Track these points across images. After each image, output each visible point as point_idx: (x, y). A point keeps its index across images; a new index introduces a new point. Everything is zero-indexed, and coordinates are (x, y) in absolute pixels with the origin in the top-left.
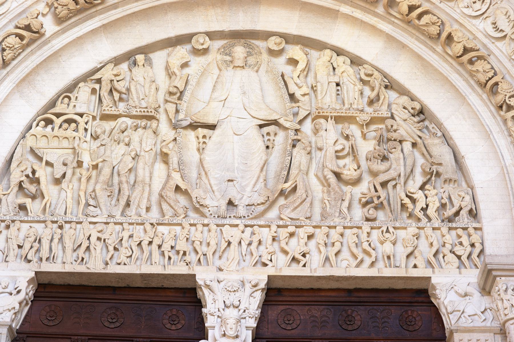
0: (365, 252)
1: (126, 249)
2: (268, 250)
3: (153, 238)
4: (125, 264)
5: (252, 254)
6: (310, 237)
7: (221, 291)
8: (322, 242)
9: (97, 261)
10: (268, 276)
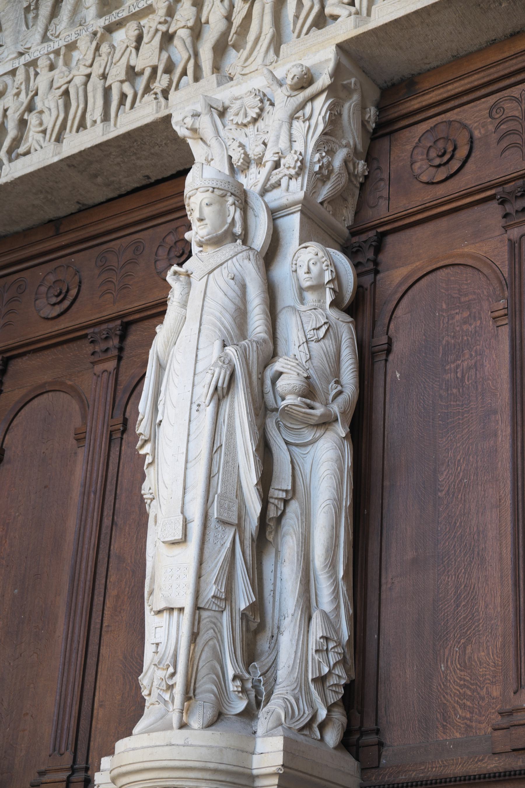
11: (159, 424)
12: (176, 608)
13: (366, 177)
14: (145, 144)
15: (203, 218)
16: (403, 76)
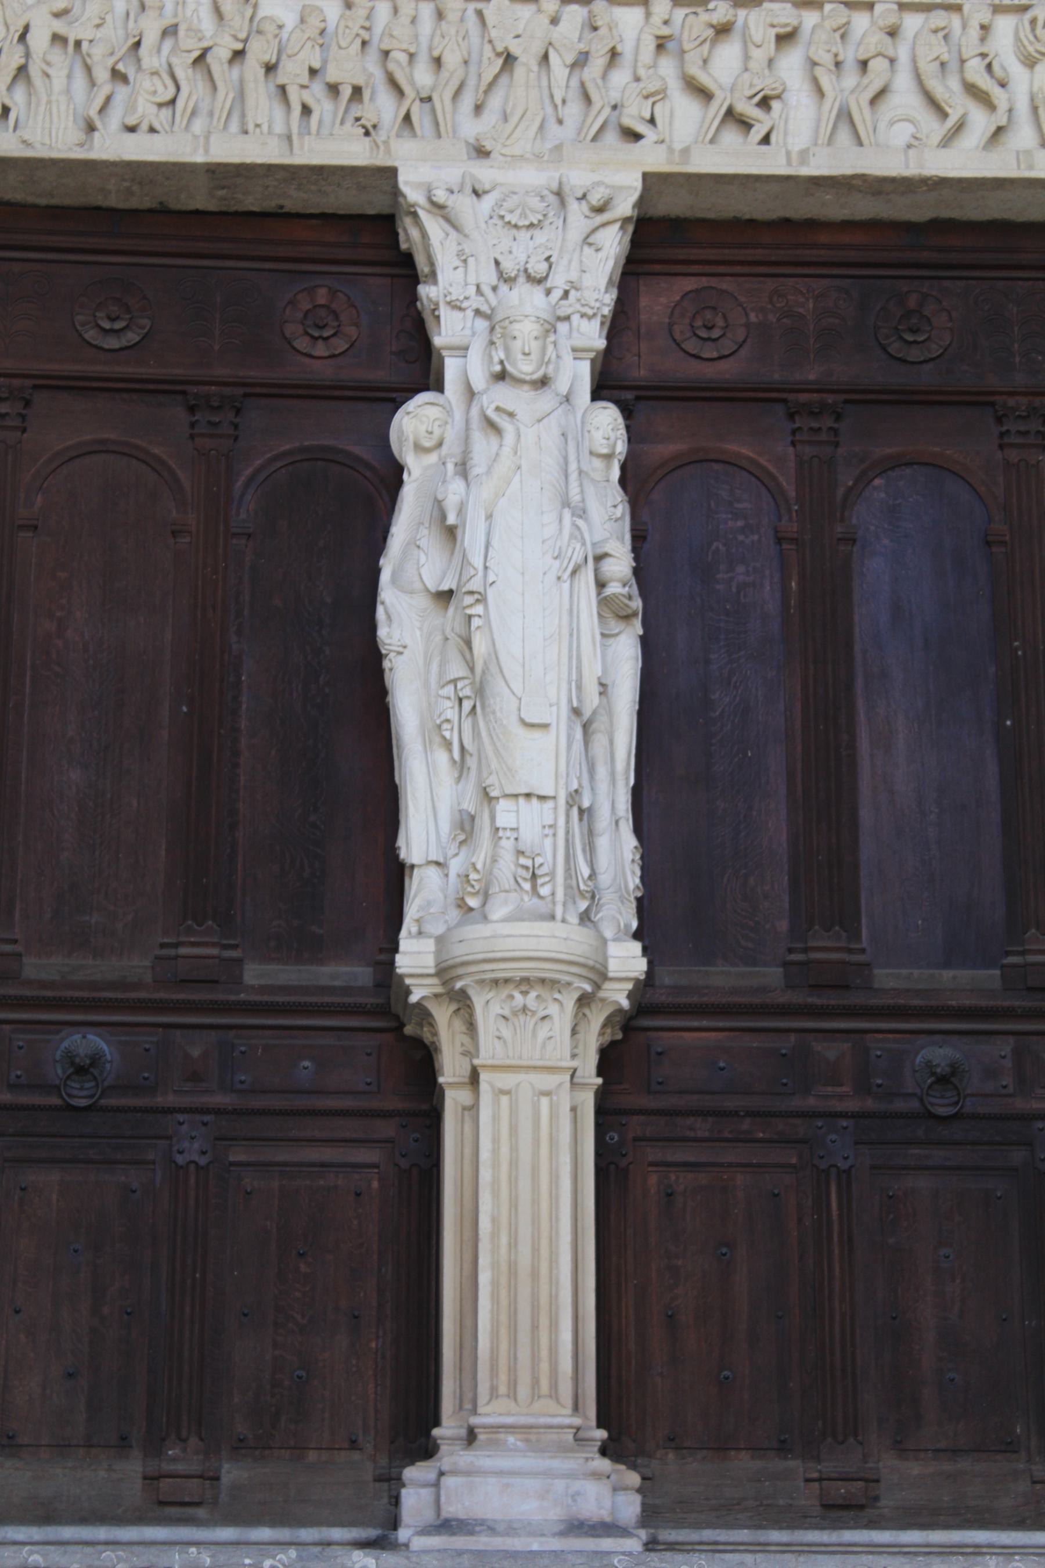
0: (972, 90)
1: (156, 79)
2: (642, 85)
3: (245, 41)
4: (152, 130)
5: (587, 99)
6: (786, 38)
7: (483, 226)
8: (827, 59)
9: (55, 119)
10: (646, 176)
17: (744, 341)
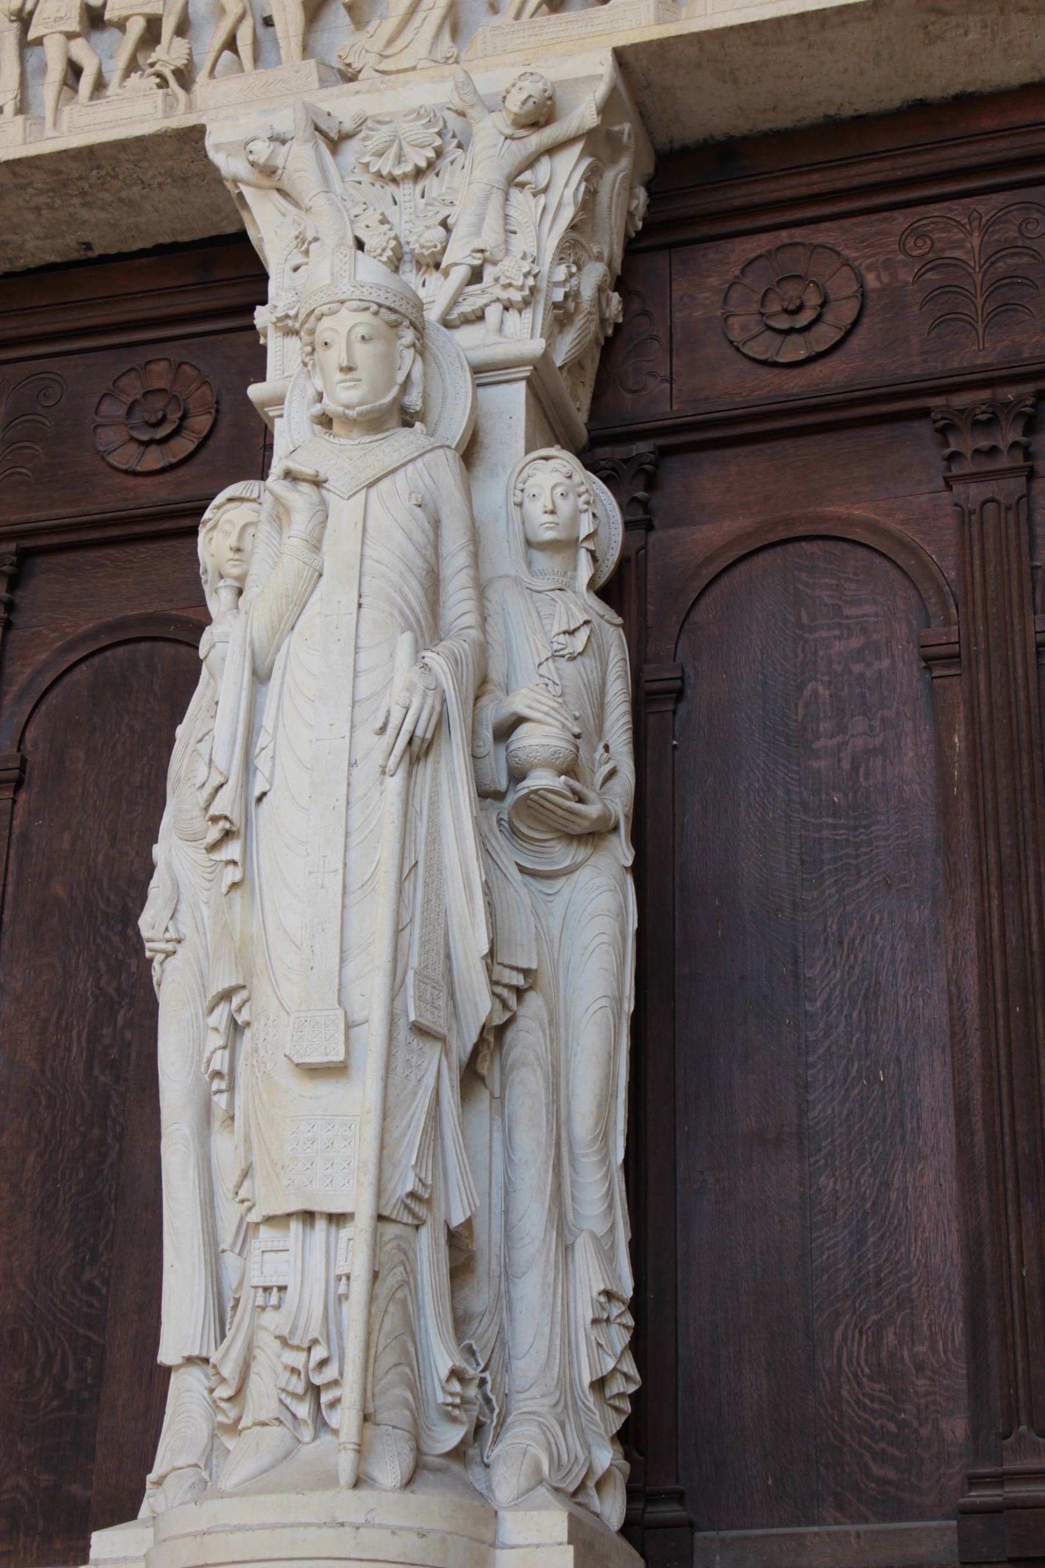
10: (619, 54)
11: (260, 799)
12: (321, 1214)
13: (617, 327)
14: (116, 176)
15: (353, 365)
16: (712, 136)
17: (856, 323)
